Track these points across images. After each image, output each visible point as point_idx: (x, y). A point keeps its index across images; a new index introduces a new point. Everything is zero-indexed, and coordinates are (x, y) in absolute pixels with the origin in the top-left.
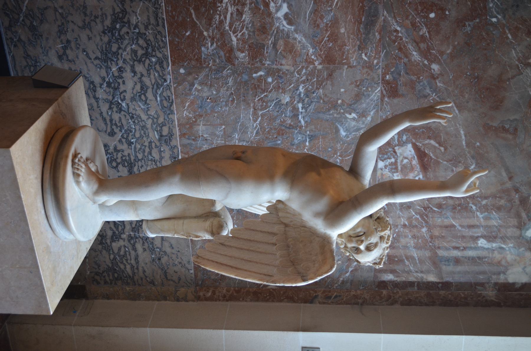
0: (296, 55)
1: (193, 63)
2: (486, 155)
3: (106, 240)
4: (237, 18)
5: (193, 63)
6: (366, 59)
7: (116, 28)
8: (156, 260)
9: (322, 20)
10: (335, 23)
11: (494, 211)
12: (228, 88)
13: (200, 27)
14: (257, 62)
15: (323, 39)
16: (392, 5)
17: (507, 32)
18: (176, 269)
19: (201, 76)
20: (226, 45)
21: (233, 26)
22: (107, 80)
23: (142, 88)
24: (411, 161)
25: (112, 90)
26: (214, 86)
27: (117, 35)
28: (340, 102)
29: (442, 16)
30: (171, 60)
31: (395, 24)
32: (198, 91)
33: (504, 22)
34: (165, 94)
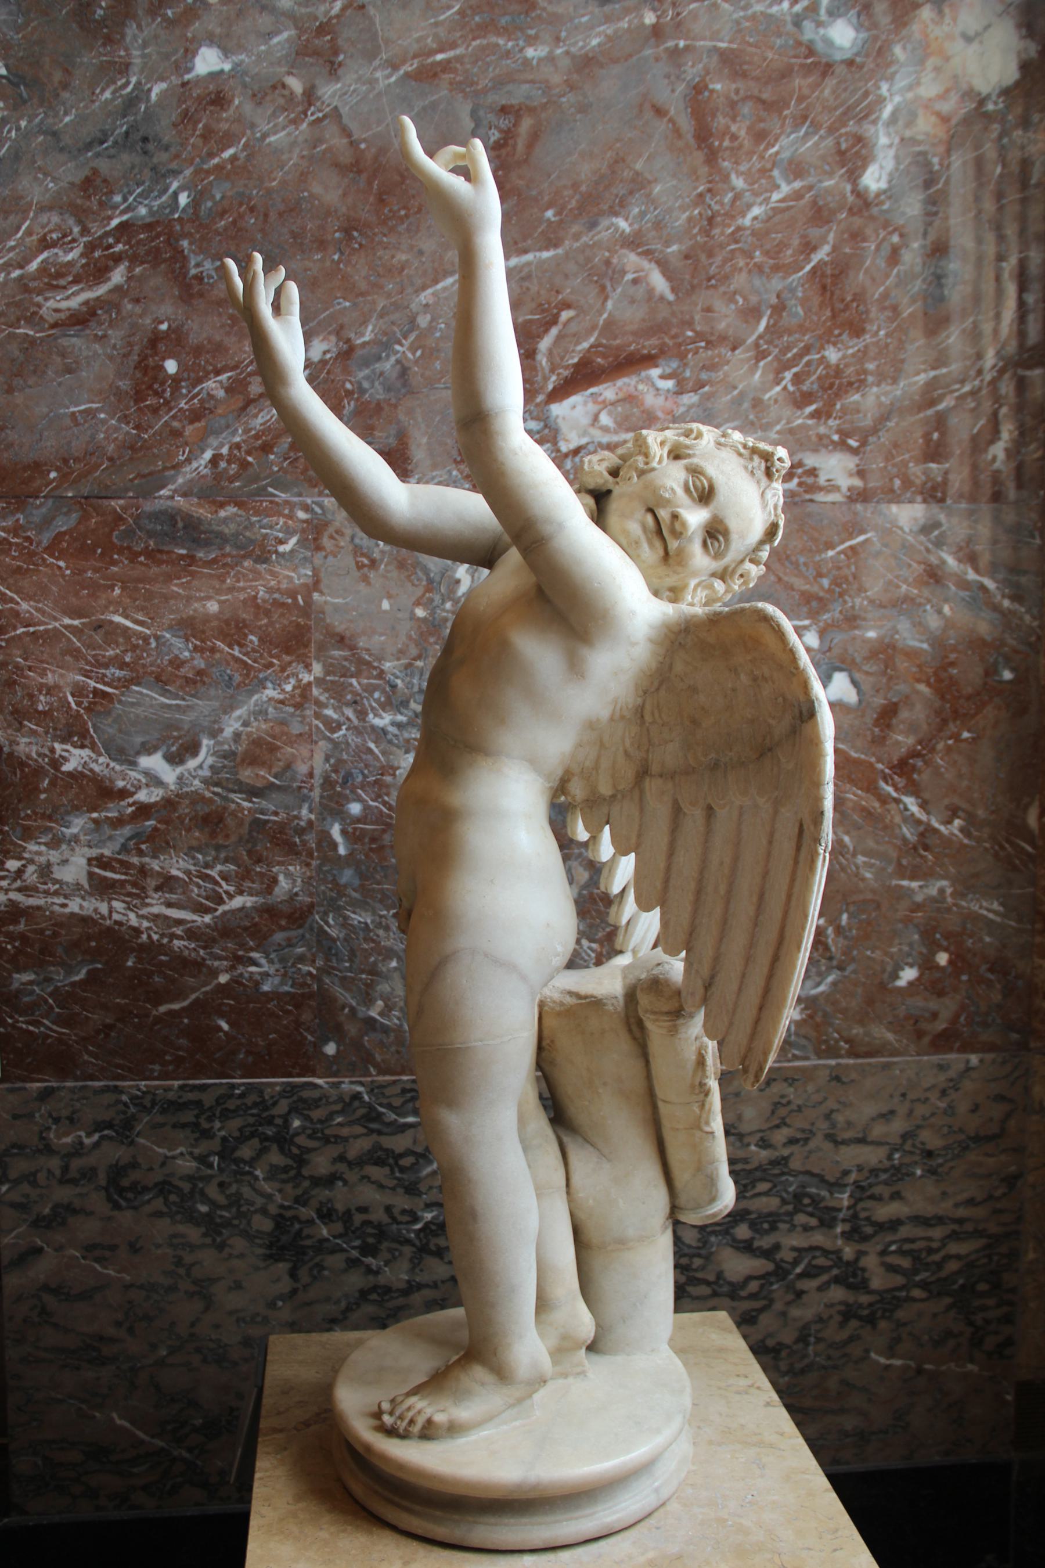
0: (283, 733)
1: (306, 1016)
2: (583, 188)
3: (860, 1306)
4: (180, 890)
5: (306, 1016)
6: (293, 540)
7: (207, 1215)
8: (934, 1163)
9: (183, 663)
10: (191, 627)
11: (766, 149)
12: (379, 925)
13: (206, 993)
14: (304, 843)
15: (237, 660)
16: (144, 476)
17: (216, 161)
18: (963, 1108)
19: (345, 997)
20: (255, 925)
21: (201, 904)
22: (355, 1253)
23: (380, 1162)
24: (605, 404)
25: (385, 1245)
26: (375, 963)
27: (226, 1214)
28: (420, 613)
29: (173, 341)
30: (299, 1075)
31: (195, 465)
32: (388, 1009)
33: (188, 172)
34: (397, 1102)
